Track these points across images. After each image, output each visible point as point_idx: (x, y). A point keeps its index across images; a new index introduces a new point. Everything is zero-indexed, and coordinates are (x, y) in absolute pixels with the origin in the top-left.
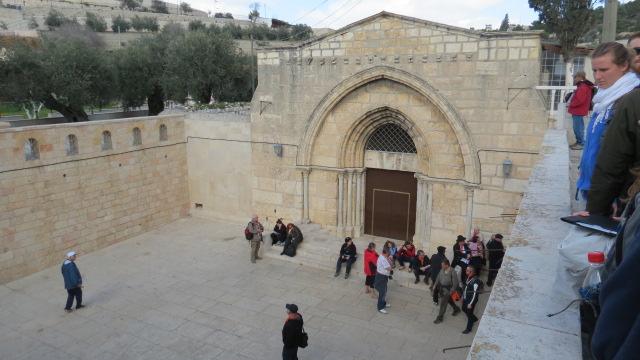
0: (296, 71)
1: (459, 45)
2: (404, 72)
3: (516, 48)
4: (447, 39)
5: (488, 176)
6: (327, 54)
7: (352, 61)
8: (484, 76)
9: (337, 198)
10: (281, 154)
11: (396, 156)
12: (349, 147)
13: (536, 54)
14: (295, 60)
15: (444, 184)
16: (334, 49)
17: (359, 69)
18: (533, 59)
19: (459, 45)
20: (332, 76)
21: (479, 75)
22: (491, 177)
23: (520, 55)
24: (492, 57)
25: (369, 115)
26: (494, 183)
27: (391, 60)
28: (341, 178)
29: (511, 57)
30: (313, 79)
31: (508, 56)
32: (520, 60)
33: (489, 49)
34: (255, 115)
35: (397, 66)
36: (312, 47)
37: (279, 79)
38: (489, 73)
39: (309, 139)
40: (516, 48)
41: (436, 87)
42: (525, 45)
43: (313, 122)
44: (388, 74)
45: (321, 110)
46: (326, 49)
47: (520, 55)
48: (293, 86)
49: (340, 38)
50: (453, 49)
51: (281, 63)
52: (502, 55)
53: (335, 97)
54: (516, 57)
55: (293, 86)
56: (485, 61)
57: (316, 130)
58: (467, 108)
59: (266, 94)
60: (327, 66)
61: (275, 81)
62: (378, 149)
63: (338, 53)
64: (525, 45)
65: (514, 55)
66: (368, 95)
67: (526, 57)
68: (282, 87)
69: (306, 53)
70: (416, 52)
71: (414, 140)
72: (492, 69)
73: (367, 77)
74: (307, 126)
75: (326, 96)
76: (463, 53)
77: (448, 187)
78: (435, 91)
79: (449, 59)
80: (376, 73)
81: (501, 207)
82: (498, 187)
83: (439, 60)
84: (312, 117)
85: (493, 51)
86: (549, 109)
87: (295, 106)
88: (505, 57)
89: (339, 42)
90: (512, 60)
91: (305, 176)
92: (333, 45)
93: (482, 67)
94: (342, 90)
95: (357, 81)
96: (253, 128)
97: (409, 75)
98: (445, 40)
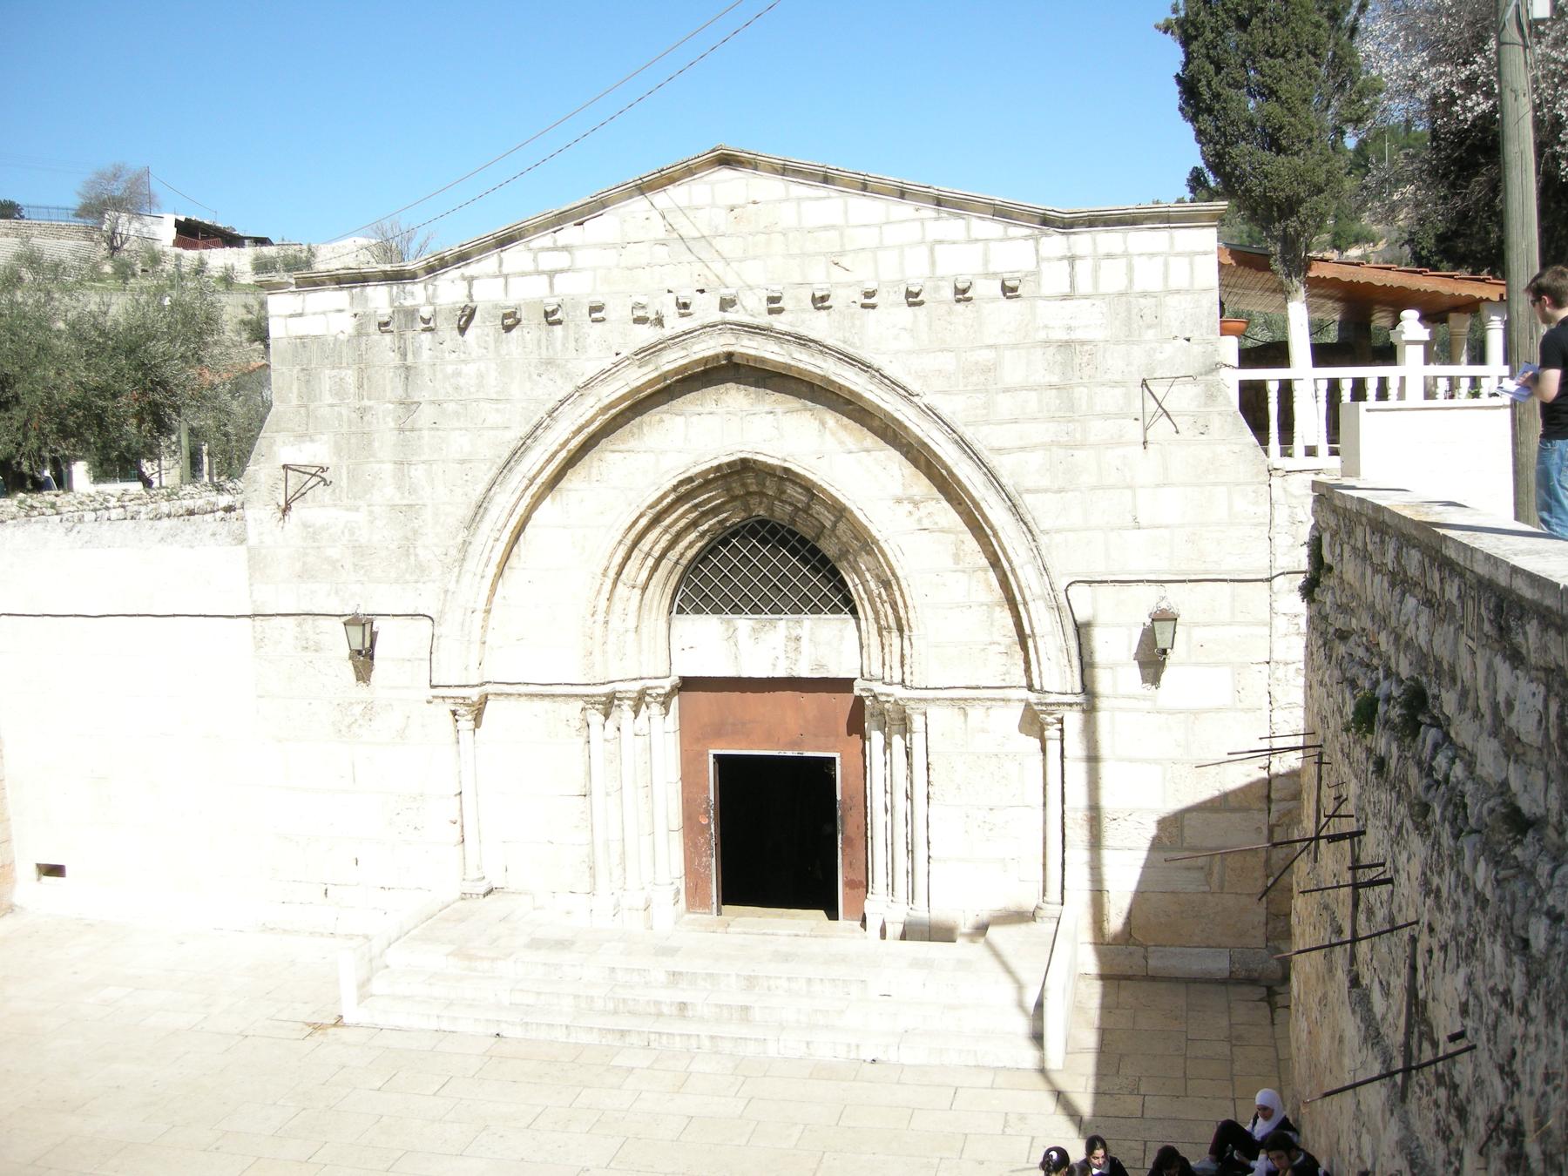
2: (803, 341)
6: (528, 292)
7: (618, 311)
8: (1066, 345)
10: (364, 659)
11: (784, 625)
12: (618, 605)
13: (1208, 274)
14: (410, 314)
15: (961, 704)
16: (552, 274)
17: (648, 334)
19: (980, 245)
20: (549, 363)
21: (1047, 343)
24: (1084, 286)
25: (687, 490)
28: (596, 718)
29: (1138, 288)
30: (481, 376)
31: (1131, 281)
33: (1072, 259)
34: (259, 515)
35: (780, 323)
36: (472, 269)
37: (350, 376)
38: (1079, 335)
39: (473, 588)
41: (914, 388)
42: (1178, 248)
43: (487, 526)
45: (517, 479)
46: (523, 274)
48: (408, 405)
49: (570, 233)
51: (360, 332)
52: (1113, 278)
53: (562, 433)
54: (1155, 285)
55: (408, 405)
56: (1065, 297)
57: (497, 556)
58: (1022, 449)
59: (303, 437)
60: (530, 332)
61: (340, 392)
62: (717, 610)
63: (566, 286)
65: (1148, 277)
66: (680, 420)
67: (1185, 284)
68: (362, 412)
69: (449, 290)
70: (838, 275)
71: (838, 565)
72: (1089, 321)
73: (672, 360)
74: (466, 543)
75: (532, 435)
77: (975, 713)
78: (908, 395)
79: (949, 294)
83: (913, 298)
84: (481, 507)
86: (1263, 439)
87: (418, 473)
88: (1121, 285)
89: (565, 248)
90: (1144, 295)
92: (550, 261)
93: (1055, 319)
94: (586, 411)
95: (637, 377)
96: (256, 563)
97: (824, 349)
98: (930, 237)
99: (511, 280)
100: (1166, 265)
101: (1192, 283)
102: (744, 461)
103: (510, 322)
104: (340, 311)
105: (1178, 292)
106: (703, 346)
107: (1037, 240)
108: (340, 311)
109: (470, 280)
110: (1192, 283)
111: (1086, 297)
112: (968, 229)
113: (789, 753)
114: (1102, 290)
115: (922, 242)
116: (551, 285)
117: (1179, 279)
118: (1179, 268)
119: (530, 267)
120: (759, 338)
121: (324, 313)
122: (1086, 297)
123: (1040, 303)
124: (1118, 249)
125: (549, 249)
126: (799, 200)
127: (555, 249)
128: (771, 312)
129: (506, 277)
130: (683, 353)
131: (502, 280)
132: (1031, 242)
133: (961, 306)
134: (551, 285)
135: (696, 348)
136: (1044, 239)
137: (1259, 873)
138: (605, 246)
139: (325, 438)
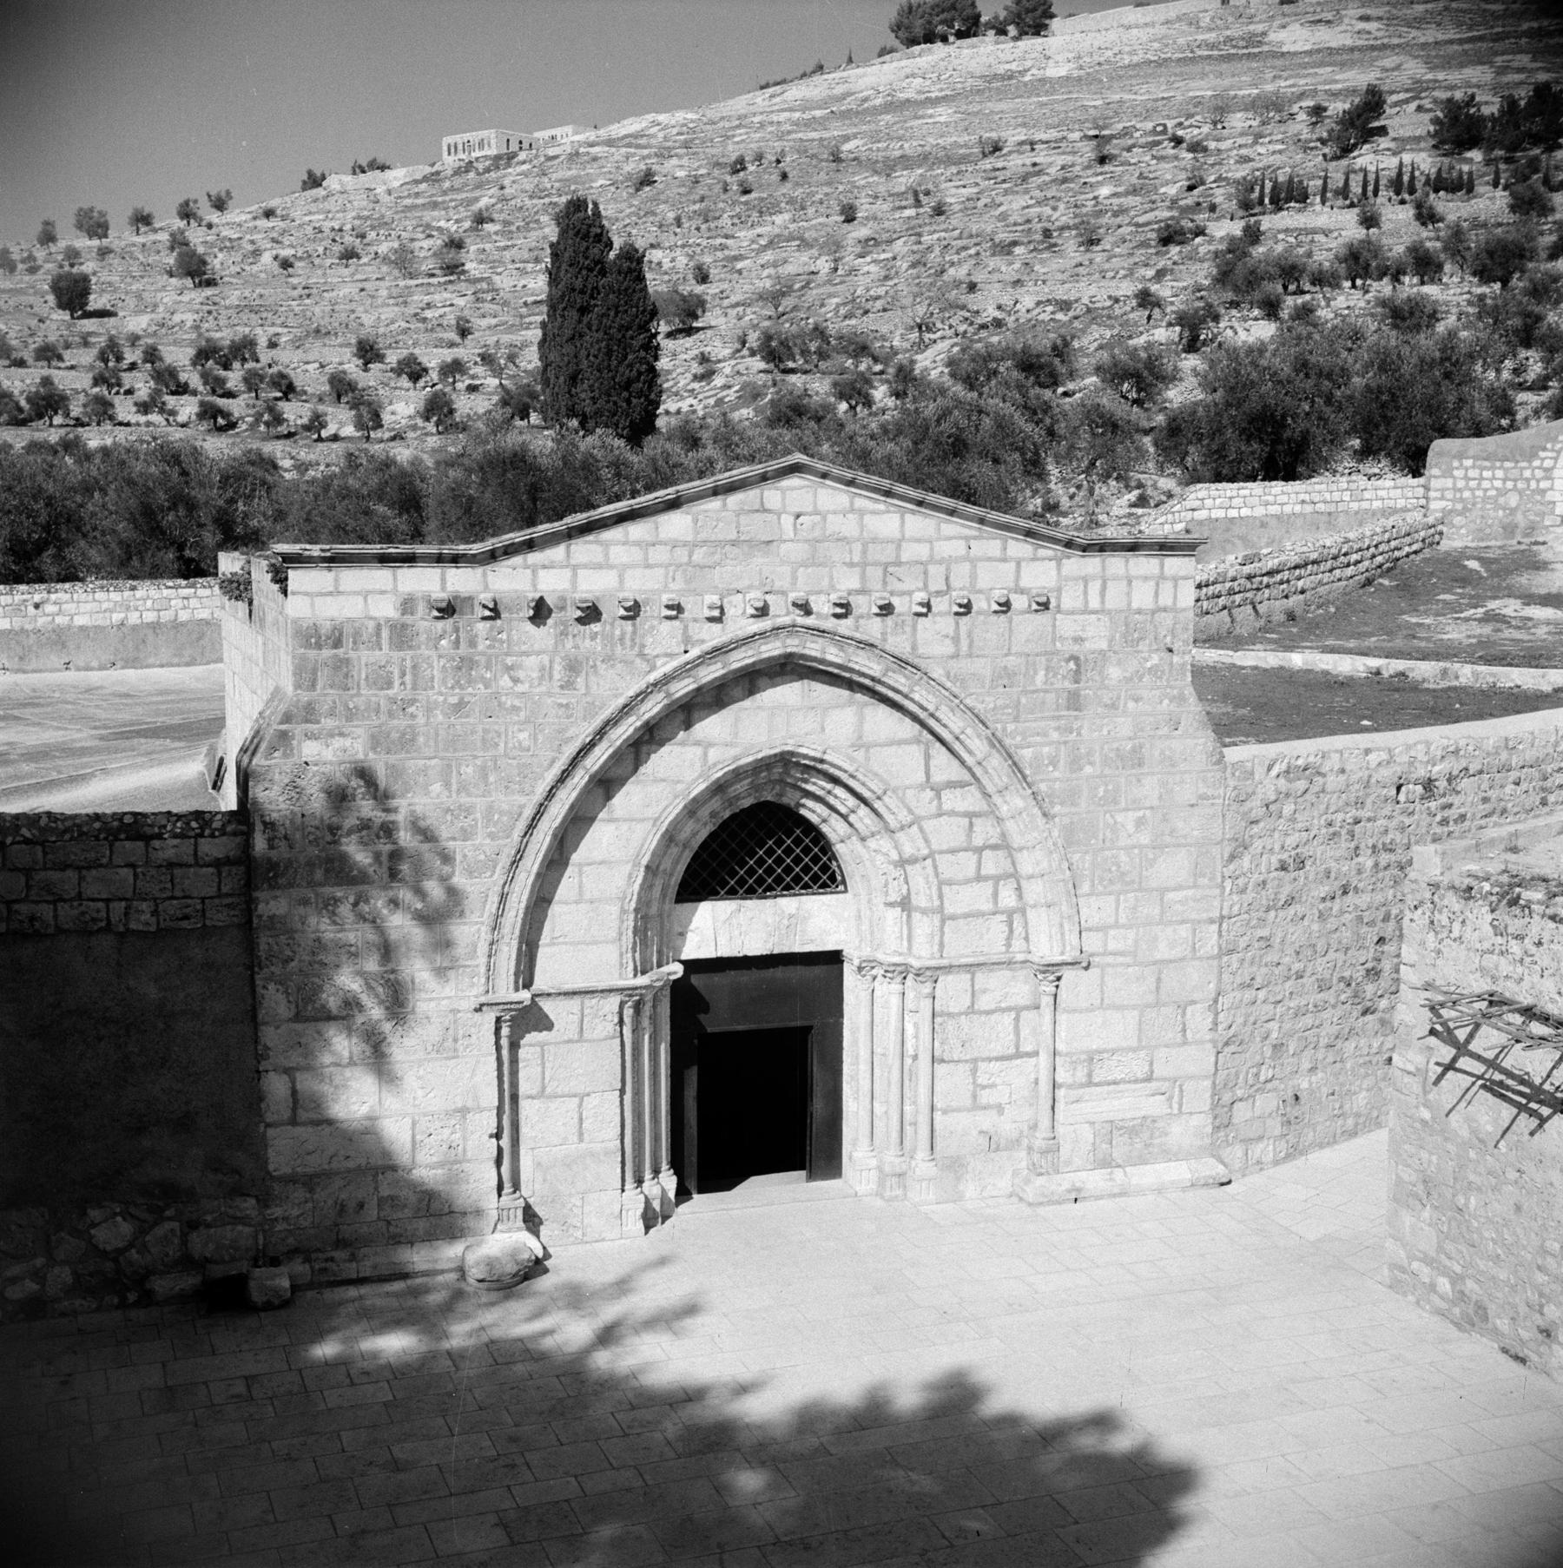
0: (472, 643)
1: (1013, 565)
3: (1146, 578)
4: (979, 548)
9: (622, 1092)
16: (622, 569)
17: (714, 636)
18: (1184, 610)
22: (1102, 929)
23: (1157, 594)
26: (1112, 946)
28: (628, 1012)
29: (1135, 605)
35: (844, 627)
40: (1146, 578)
44: (814, 648)
47: (1157, 594)
50: (993, 580)
52: (1115, 598)
67: (1169, 603)
72: (1097, 635)
73: (740, 659)
80: (772, 649)
81: (1134, 1007)
82: (1122, 954)
85: (1095, 587)
90: (1139, 612)
91: (505, 1031)
93: (1067, 626)
101: (1175, 603)
102: (782, 754)
103: (591, 614)
104: (383, 592)
105: (1165, 610)
106: (769, 646)
107: (1059, 561)
108: (383, 592)
110: (1175, 603)
113: (740, 1028)
114: (1108, 606)
115: (966, 558)
116: (621, 581)
117: (1166, 599)
119: (600, 558)
120: (820, 640)
121: (366, 594)
124: (1122, 572)
125: (618, 543)
126: (862, 513)
128: (837, 616)
129: (575, 568)
130: (750, 653)
131: (567, 573)
133: (994, 618)
134: (621, 581)
135: (763, 648)
137: (1208, 1094)
139: (359, 731)
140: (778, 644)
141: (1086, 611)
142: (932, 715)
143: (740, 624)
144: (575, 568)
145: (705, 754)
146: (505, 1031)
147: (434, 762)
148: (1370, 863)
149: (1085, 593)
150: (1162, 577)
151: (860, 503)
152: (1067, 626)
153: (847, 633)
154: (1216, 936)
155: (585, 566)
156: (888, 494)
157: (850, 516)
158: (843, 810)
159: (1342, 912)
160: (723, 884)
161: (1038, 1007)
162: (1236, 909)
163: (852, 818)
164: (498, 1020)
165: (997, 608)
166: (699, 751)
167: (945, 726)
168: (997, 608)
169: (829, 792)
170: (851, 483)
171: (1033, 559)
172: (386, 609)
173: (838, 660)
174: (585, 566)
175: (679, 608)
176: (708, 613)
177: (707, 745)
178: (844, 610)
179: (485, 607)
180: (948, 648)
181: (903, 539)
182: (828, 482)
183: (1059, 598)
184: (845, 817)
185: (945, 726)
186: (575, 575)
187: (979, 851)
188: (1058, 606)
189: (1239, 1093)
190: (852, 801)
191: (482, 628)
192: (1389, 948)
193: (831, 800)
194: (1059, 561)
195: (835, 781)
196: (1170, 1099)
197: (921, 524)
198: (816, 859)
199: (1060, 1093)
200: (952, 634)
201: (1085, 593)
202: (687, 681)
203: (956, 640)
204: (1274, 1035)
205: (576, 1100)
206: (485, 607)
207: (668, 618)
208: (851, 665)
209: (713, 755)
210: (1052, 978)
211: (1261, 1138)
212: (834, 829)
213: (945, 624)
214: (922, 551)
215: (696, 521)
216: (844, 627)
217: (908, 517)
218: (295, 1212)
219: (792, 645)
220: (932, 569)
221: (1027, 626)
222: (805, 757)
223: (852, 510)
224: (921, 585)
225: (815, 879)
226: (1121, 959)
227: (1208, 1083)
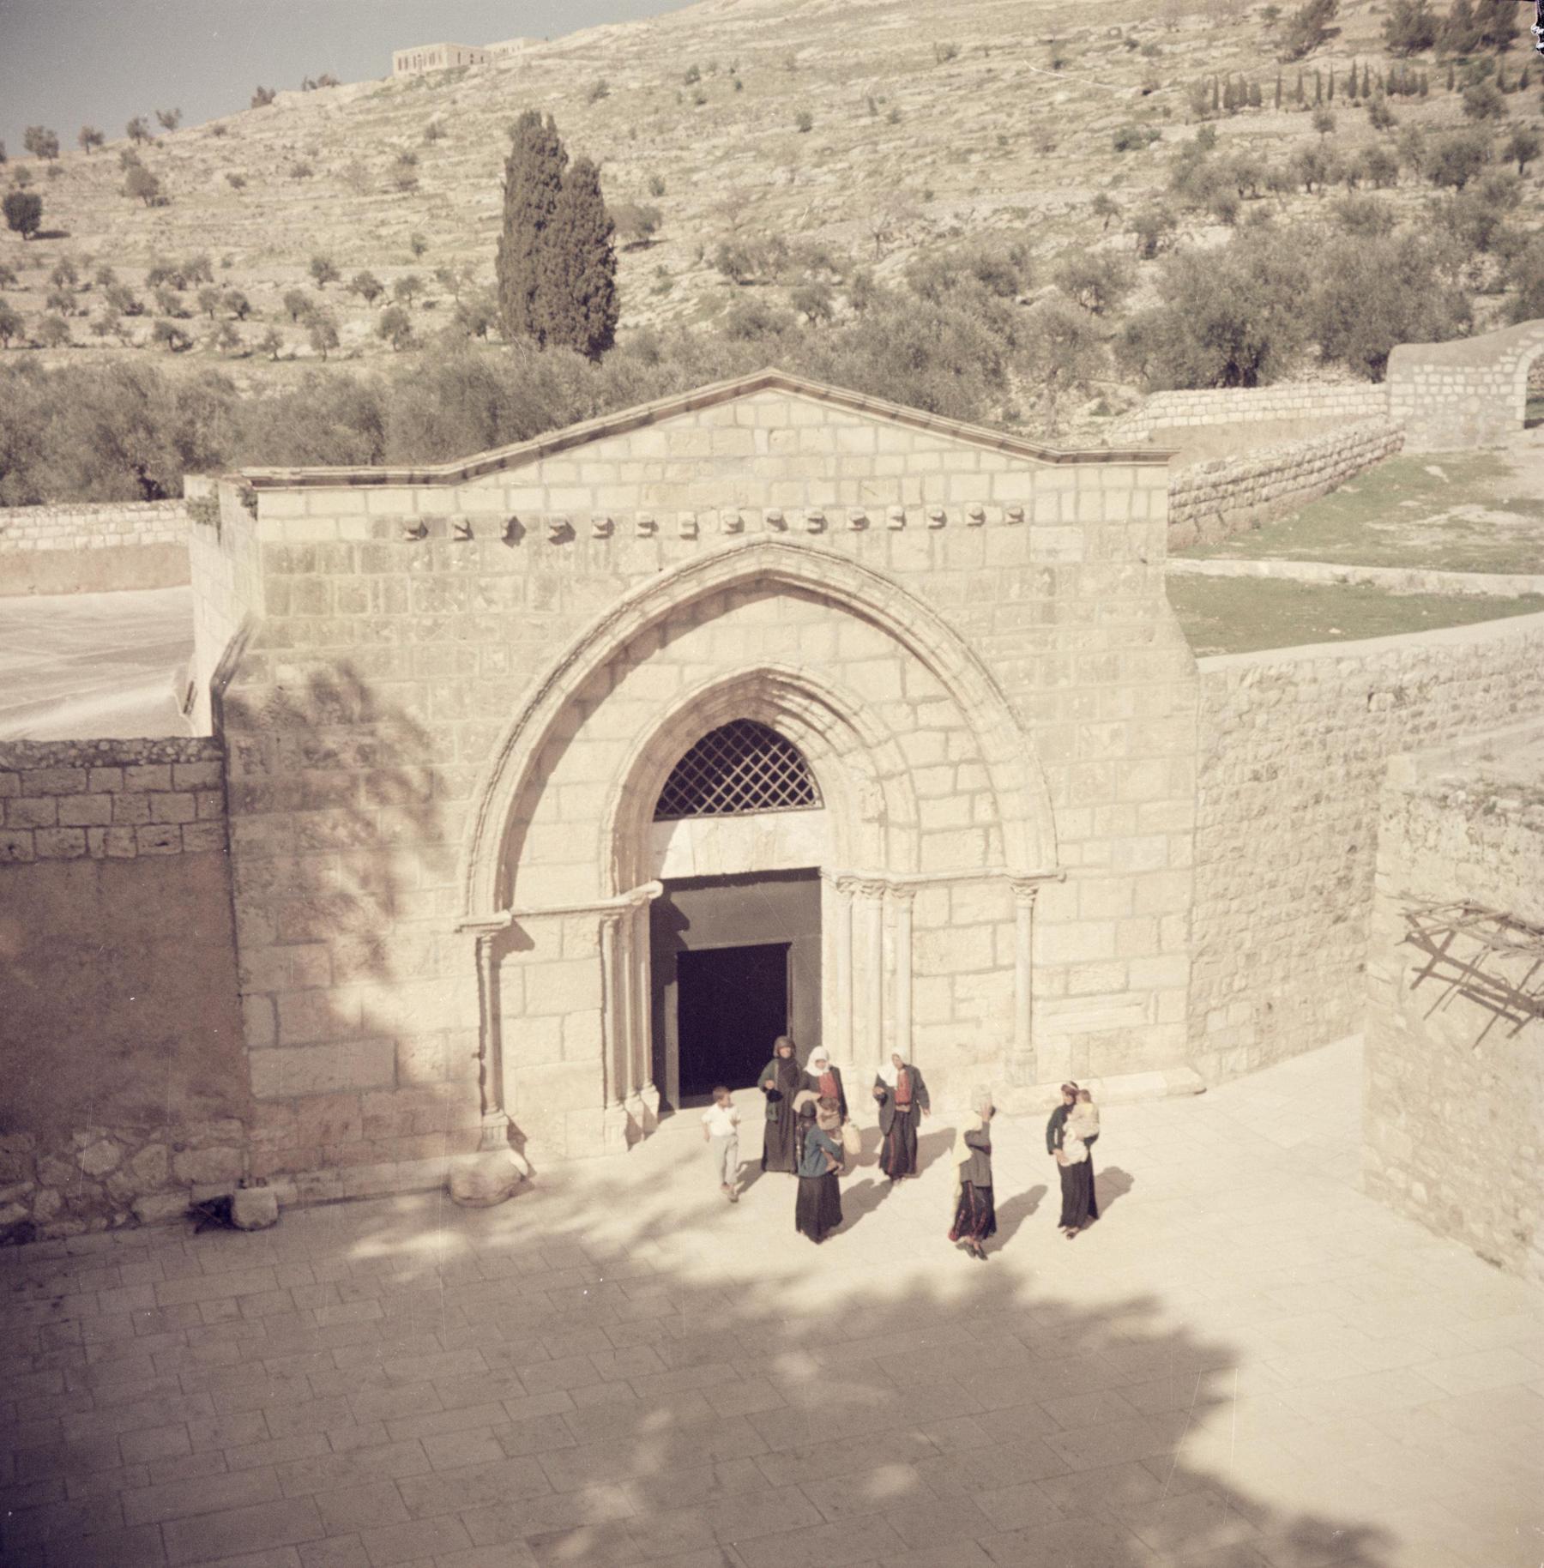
0: (445, 564)
1: (986, 478)
3: (1119, 489)
4: (950, 461)
5: (1074, 842)
9: (603, 1010)
17: (689, 553)
23: (1130, 505)
27: (798, 522)
28: (608, 932)
29: (1109, 517)
32: (1133, 521)
40: (1119, 489)
44: (788, 564)
47: (1130, 505)
50: (967, 493)
54: (1122, 515)
64: (1140, 483)
72: (1071, 545)
73: (716, 577)
76: (995, 504)
80: (747, 566)
90: (1113, 523)
91: (486, 952)
93: (1041, 538)
99: (553, 492)
100: (1131, 495)
101: (1149, 513)
104: (353, 515)
105: (1139, 521)
106: (745, 563)
107: (1032, 472)
109: (507, 489)
110: (1149, 513)
111: (1070, 524)
112: (978, 461)
117: (1139, 510)
118: (1140, 499)
120: (796, 556)
121: (336, 517)
122: (1070, 524)
123: (1033, 529)
126: (835, 427)
127: (597, 461)
129: (547, 488)
132: (1027, 475)
133: (968, 531)
134: (594, 496)
135: (738, 565)
136: (1039, 473)
137: (1182, 1005)
138: (647, 462)
140: (753, 560)
141: (1060, 523)
142: (908, 630)
143: (715, 541)
144: (547, 488)
145: (681, 672)
146: (486, 952)
147: (408, 685)
148: (1341, 772)
149: (1059, 505)
150: (1136, 487)
151: (834, 417)
152: (1041, 538)
153: (824, 549)
154: (1190, 847)
155: (557, 486)
156: (862, 407)
157: (825, 430)
158: (820, 726)
159: (1314, 822)
160: (701, 802)
161: (1014, 921)
162: (1210, 818)
163: (829, 735)
164: (479, 941)
165: (971, 520)
166: (675, 669)
167: (921, 641)
168: (971, 520)
169: (806, 709)
170: (825, 397)
171: (1008, 471)
172: (358, 532)
173: (814, 577)
174: (557, 486)
175: (653, 526)
176: (682, 531)
177: (683, 664)
178: (820, 525)
179: (458, 528)
180: (922, 562)
181: (877, 453)
182: (801, 396)
183: (1033, 511)
184: (822, 734)
185: (921, 641)
186: (547, 495)
187: (955, 765)
188: (1032, 518)
189: (1213, 1003)
190: (829, 717)
191: (455, 548)
192: (1362, 856)
193: (807, 716)
194: (1032, 472)
195: (812, 697)
196: (1146, 1009)
197: (894, 437)
198: (793, 776)
199: (1038, 1005)
200: (926, 547)
201: (1059, 505)
202: (661, 600)
203: (931, 554)
204: (1247, 945)
205: (557, 1020)
206: (458, 528)
207: (642, 536)
208: (827, 581)
209: (689, 673)
210: (1029, 891)
211: (1235, 1046)
212: (809, 746)
213: (916, 537)
214: (896, 465)
215: (668, 438)
216: (820, 542)
217: (882, 430)
218: (280, 1134)
219: (767, 562)
220: (905, 482)
221: (1001, 538)
222: (782, 674)
223: (826, 424)
224: (895, 498)
225: (793, 795)
226: (1096, 872)
227: (1183, 993)
